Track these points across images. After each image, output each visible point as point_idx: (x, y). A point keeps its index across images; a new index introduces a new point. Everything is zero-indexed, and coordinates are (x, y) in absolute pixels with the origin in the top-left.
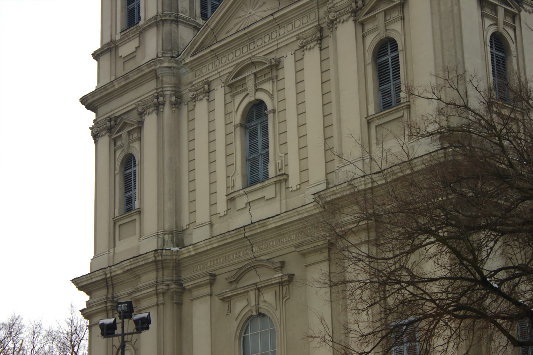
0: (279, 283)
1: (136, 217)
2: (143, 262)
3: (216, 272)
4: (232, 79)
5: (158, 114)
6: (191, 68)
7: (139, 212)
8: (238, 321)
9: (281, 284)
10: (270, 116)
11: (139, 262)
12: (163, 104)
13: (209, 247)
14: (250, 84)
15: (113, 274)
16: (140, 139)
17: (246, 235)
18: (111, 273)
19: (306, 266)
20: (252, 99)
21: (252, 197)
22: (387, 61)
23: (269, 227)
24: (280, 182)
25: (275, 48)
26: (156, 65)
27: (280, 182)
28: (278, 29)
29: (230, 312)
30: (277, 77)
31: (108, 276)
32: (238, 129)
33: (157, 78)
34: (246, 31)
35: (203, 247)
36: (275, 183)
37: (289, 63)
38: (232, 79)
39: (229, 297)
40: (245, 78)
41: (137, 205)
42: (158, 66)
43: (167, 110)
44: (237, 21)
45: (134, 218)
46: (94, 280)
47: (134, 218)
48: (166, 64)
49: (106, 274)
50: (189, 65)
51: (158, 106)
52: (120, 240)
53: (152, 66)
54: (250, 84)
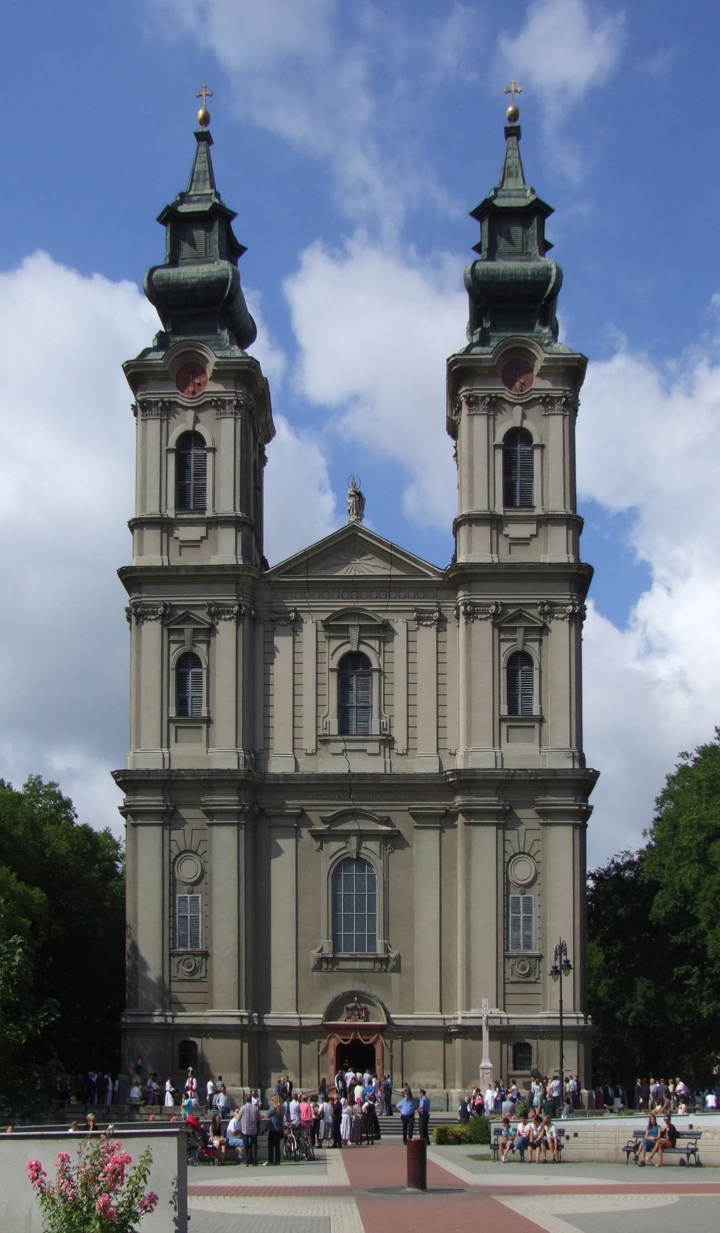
0: (385, 835)
6: (272, 588)
8: (333, 859)
11: (223, 776)
13: (305, 782)
14: (354, 634)
15: (179, 778)
17: (352, 782)
18: (177, 776)
20: (355, 649)
21: (350, 746)
23: (381, 782)
26: (243, 572)
28: (388, 591)
31: (173, 778)
33: (237, 584)
35: (296, 780)
39: (324, 835)
42: (245, 573)
46: (151, 778)
48: (253, 575)
49: (170, 776)
50: (272, 583)
52: (176, 742)
53: (239, 570)
54: (354, 634)
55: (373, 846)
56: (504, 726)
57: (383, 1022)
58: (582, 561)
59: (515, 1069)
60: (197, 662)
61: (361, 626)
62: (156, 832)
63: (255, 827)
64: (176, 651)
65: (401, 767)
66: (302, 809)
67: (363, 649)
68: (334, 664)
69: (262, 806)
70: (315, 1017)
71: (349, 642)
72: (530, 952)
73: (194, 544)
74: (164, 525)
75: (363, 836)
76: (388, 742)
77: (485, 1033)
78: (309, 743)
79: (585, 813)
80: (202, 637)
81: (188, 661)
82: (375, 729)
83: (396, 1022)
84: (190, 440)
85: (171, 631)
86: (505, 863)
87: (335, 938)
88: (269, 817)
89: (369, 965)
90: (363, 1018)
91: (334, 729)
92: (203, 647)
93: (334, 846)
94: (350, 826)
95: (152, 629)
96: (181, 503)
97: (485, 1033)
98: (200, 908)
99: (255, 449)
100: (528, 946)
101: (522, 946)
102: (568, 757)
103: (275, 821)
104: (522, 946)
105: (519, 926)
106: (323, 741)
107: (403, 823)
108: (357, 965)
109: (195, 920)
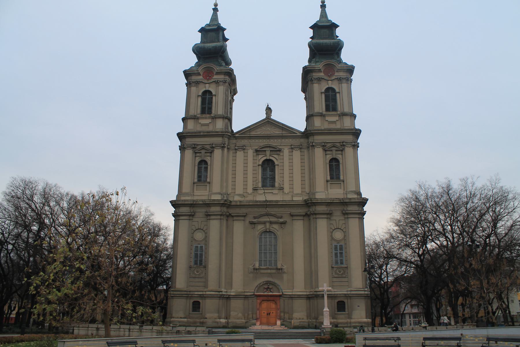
1: (208, 184)
2: (217, 203)
3: (247, 213)
4: (260, 149)
5: (222, 150)
7: (209, 183)
8: (259, 232)
9: (281, 223)
10: (276, 167)
12: (225, 147)
14: (268, 153)
16: (211, 156)
17: (267, 204)
19: (293, 220)
22: (333, 164)
24: (280, 189)
25: (280, 145)
27: (280, 189)
29: (254, 228)
30: (280, 154)
32: (260, 167)
34: (268, 135)
36: (278, 189)
37: (286, 151)
38: (260, 149)
40: (265, 150)
41: (208, 180)
43: (226, 149)
44: (262, 130)
45: (206, 184)
47: (206, 184)
51: (223, 148)
54: (268, 153)
55: (276, 226)
56: (329, 185)
57: (281, 294)
58: (357, 127)
59: (338, 311)
60: (205, 162)
61: (271, 150)
62: (187, 222)
63: (227, 220)
64: (198, 159)
65: (288, 198)
66: (246, 214)
67: (271, 158)
68: (260, 163)
69: (230, 213)
70: (250, 290)
71: (266, 156)
72: (343, 266)
73: (207, 125)
74: (195, 118)
75: (271, 223)
76: (281, 189)
77: (326, 297)
78: (250, 190)
79: (364, 213)
80: (208, 154)
81: (203, 162)
82: (277, 185)
83: (284, 293)
84: (207, 93)
85: (196, 153)
86: (331, 232)
87: (260, 261)
88: (233, 216)
89: (274, 271)
90: (271, 292)
91: (260, 185)
92: (209, 158)
93: (260, 227)
94: (266, 219)
95: (189, 153)
96: (203, 111)
97: (326, 297)
98: (204, 250)
99: (230, 96)
100: (342, 263)
101: (339, 263)
102: (355, 194)
103: (235, 218)
104: (339, 263)
105: (337, 256)
106: (255, 189)
107: (286, 218)
108: (269, 271)
109: (201, 255)
